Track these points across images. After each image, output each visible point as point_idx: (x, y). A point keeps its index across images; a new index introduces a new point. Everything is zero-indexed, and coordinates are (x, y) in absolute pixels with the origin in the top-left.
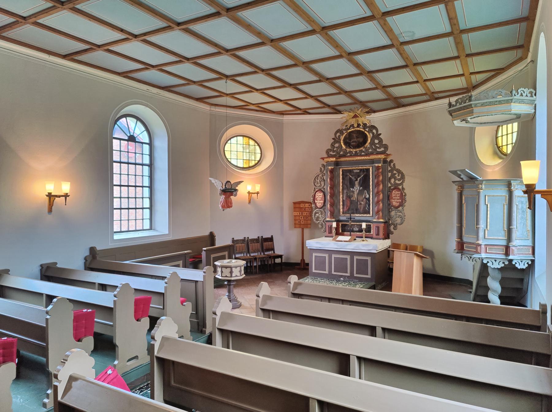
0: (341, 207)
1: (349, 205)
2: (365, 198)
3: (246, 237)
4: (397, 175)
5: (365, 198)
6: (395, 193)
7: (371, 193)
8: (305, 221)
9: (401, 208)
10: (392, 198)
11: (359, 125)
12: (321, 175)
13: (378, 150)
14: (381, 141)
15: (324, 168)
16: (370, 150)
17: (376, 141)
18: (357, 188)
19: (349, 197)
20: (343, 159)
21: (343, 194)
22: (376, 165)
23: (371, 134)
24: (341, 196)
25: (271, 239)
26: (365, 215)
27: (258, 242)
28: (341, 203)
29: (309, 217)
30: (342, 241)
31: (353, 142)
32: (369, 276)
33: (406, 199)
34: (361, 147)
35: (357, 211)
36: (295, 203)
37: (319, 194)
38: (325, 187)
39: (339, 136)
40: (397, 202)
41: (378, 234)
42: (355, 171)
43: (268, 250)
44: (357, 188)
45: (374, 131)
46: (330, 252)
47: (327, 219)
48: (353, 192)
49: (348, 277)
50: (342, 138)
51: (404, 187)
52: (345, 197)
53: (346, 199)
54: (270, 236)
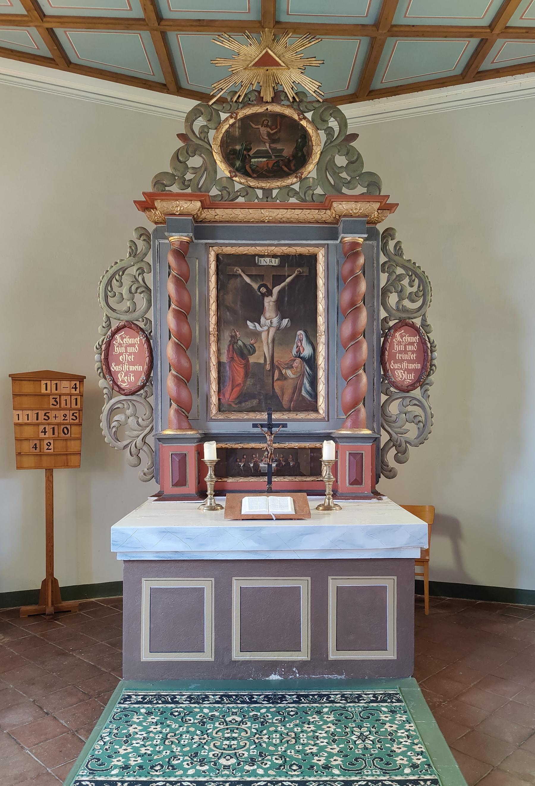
0: (214, 387)
1: (239, 379)
2: (299, 356)
4: (406, 282)
5: (299, 356)
6: (403, 342)
7: (322, 339)
9: (417, 393)
10: (393, 357)
11: (278, 96)
12: (133, 270)
13: (345, 190)
14: (355, 160)
15: (148, 240)
16: (319, 191)
17: (341, 161)
18: (270, 320)
19: (243, 353)
20: (221, 214)
21: (218, 340)
22: (349, 238)
23: (322, 133)
24: (213, 348)
26: (302, 415)
28: (214, 374)
30: (268, 518)
31: (259, 154)
32: (390, 654)
33: (435, 362)
34: (286, 175)
35: (271, 402)
36: (16, 378)
37: (128, 340)
38: (150, 315)
39: (204, 130)
40: (409, 371)
41: (357, 481)
42: (263, 262)
44: (270, 320)
45: (333, 123)
46: (224, 569)
47: (168, 432)
48: (257, 335)
49: (302, 665)
50: (215, 137)
51: (429, 322)
52: (224, 351)
53: (232, 359)
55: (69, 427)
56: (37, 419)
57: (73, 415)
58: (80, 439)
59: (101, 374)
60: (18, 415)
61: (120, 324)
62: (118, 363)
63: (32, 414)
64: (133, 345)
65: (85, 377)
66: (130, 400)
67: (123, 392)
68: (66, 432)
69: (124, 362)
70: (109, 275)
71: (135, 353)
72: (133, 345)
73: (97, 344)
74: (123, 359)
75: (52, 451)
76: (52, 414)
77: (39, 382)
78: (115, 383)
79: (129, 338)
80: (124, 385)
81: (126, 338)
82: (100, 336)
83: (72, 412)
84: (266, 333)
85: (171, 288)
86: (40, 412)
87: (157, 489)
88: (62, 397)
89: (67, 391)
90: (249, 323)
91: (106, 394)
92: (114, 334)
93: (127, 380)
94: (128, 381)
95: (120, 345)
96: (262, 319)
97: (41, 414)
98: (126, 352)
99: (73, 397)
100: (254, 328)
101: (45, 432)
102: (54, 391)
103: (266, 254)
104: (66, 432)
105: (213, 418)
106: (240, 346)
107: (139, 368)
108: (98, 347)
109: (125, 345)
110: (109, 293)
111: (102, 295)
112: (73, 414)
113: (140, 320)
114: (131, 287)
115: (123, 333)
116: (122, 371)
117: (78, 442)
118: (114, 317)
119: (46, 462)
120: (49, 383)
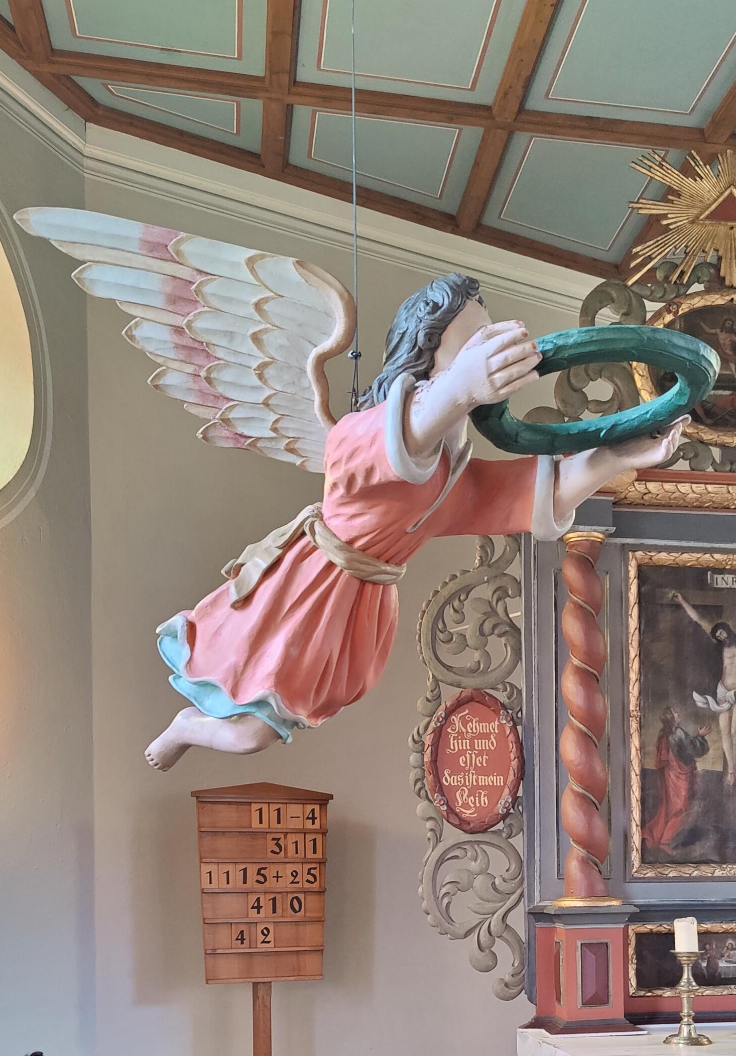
12: (485, 592)
29: (311, 902)
36: (199, 796)
37: (475, 726)
38: (519, 679)
48: (709, 718)
55: (301, 896)
56: (245, 882)
57: (309, 873)
58: (320, 921)
60: (210, 873)
61: (463, 695)
62: (457, 770)
64: (487, 736)
65: (331, 797)
66: (479, 842)
68: (297, 907)
69: (467, 768)
70: (441, 599)
71: (488, 752)
72: (487, 736)
74: (466, 763)
75: (272, 944)
76: (270, 872)
77: (246, 807)
78: (451, 810)
79: (479, 722)
80: (467, 813)
81: (472, 721)
83: (307, 867)
84: (727, 714)
85: (572, 627)
86: (248, 866)
87: (530, 1012)
88: (288, 835)
89: (297, 824)
90: (695, 695)
91: (432, 830)
93: (475, 803)
95: (460, 735)
96: (720, 690)
97: (252, 870)
99: (310, 837)
100: (705, 706)
101: (258, 908)
102: (274, 824)
103: (728, 567)
104: (297, 907)
105: (636, 875)
106: (681, 740)
107: (496, 780)
108: (416, 737)
109: (469, 735)
110: (438, 632)
111: (426, 637)
112: (309, 870)
113: (500, 686)
114: (482, 625)
115: (467, 711)
117: (317, 926)
118: (449, 681)
120: (265, 807)
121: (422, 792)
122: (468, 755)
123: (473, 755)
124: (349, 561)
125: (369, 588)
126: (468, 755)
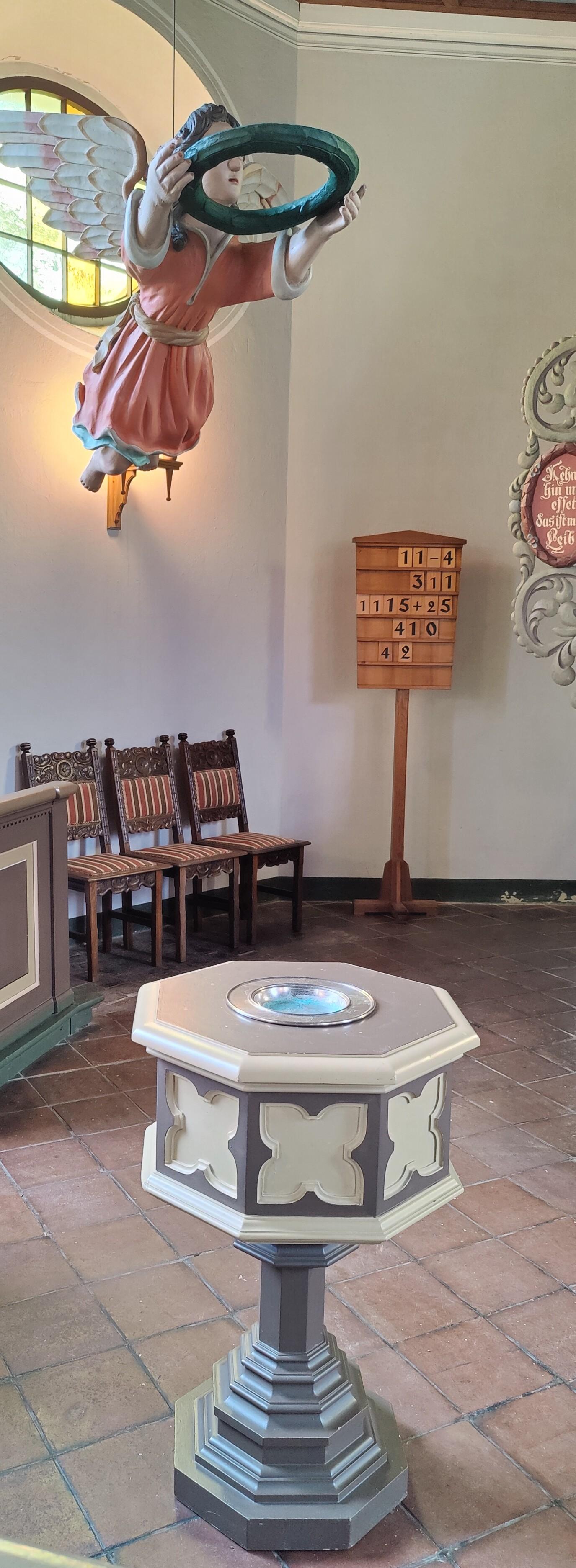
3: (100, 739)
8: (423, 650)
25: (224, 753)
27: (162, 771)
43: (214, 814)
54: (216, 735)
55: (436, 622)
56: (391, 610)
57: (444, 604)
58: (451, 642)
59: (518, 533)
61: (557, 448)
62: (548, 513)
63: (383, 601)
65: (465, 542)
66: (564, 576)
67: (555, 562)
68: (432, 631)
69: (558, 512)
70: (543, 365)
73: (515, 482)
75: (410, 660)
76: (412, 601)
77: (395, 550)
78: (541, 547)
80: (555, 551)
81: (564, 470)
82: (518, 470)
83: (442, 599)
86: (395, 598)
88: (428, 574)
89: (436, 564)
91: (524, 565)
92: (545, 464)
94: (563, 544)
95: (554, 483)
97: (397, 600)
98: (564, 494)
99: (446, 575)
101: (401, 630)
102: (417, 564)
104: (432, 631)
108: (515, 487)
109: (561, 483)
110: (540, 395)
111: (529, 398)
112: (444, 601)
115: (561, 462)
116: (555, 526)
117: (448, 647)
118: (547, 436)
119: (401, 677)
120: (409, 550)
121: (518, 533)
122: (559, 501)
123: (564, 501)
124: (152, 331)
125: (175, 350)
126: (559, 501)
